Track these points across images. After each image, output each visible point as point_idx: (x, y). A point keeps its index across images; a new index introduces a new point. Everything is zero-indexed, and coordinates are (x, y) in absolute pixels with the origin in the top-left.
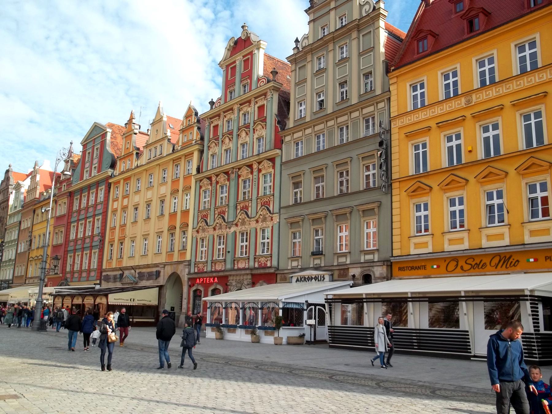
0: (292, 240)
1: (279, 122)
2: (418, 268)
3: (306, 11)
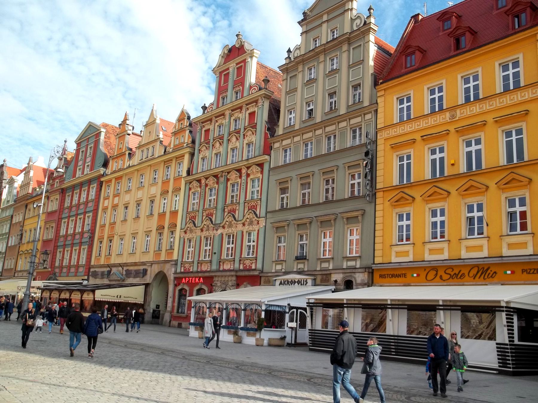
0: (277, 244)
1: (269, 129)
2: (399, 276)
3: (299, 23)
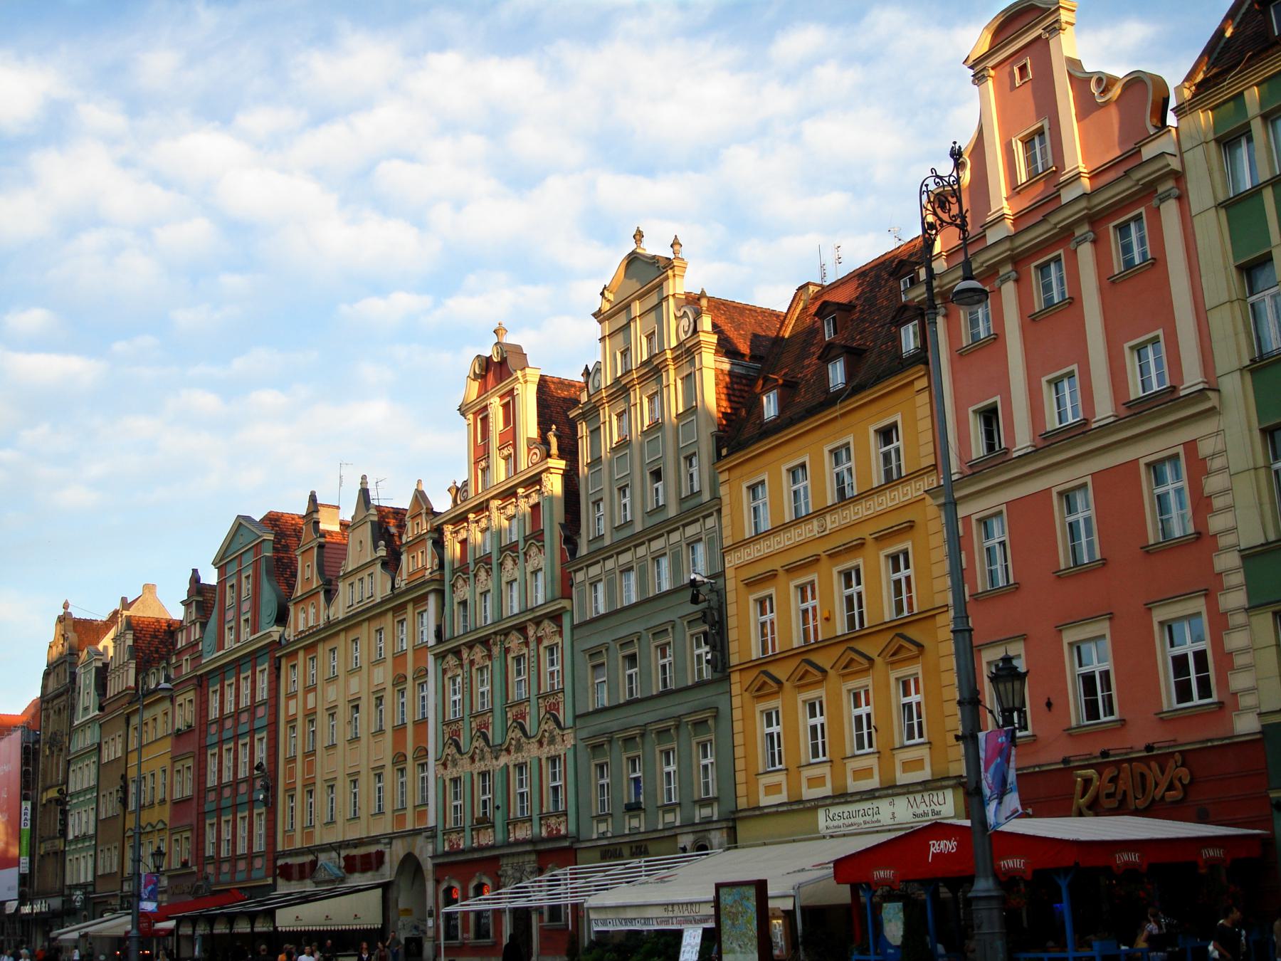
0: (597, 780)
